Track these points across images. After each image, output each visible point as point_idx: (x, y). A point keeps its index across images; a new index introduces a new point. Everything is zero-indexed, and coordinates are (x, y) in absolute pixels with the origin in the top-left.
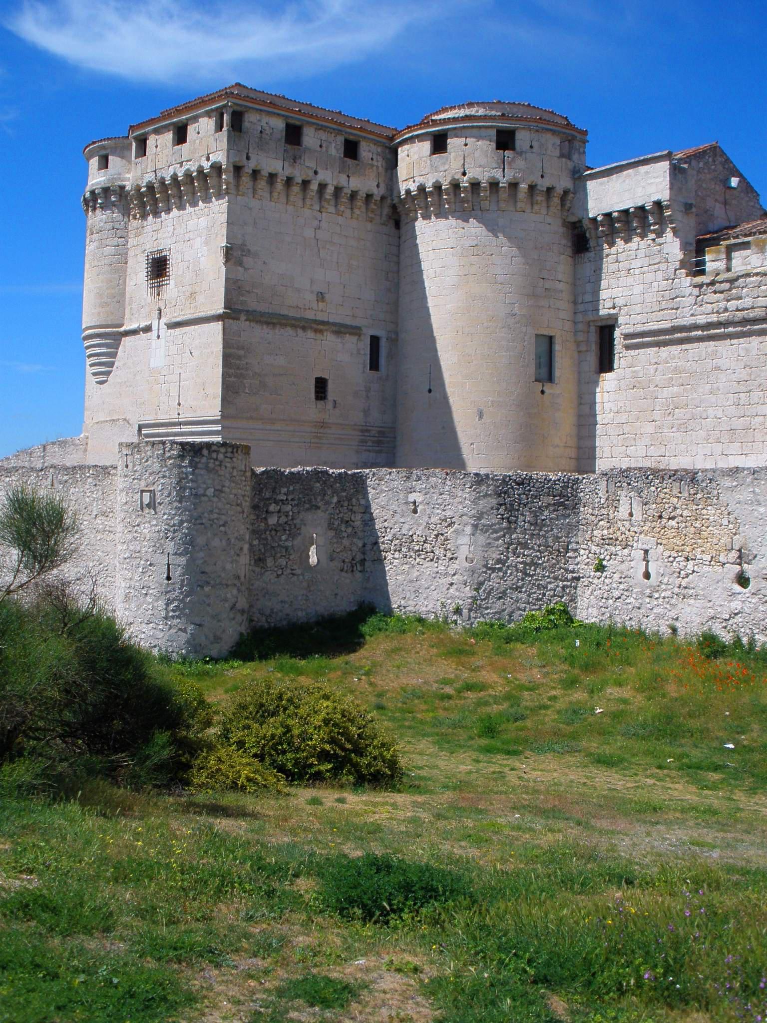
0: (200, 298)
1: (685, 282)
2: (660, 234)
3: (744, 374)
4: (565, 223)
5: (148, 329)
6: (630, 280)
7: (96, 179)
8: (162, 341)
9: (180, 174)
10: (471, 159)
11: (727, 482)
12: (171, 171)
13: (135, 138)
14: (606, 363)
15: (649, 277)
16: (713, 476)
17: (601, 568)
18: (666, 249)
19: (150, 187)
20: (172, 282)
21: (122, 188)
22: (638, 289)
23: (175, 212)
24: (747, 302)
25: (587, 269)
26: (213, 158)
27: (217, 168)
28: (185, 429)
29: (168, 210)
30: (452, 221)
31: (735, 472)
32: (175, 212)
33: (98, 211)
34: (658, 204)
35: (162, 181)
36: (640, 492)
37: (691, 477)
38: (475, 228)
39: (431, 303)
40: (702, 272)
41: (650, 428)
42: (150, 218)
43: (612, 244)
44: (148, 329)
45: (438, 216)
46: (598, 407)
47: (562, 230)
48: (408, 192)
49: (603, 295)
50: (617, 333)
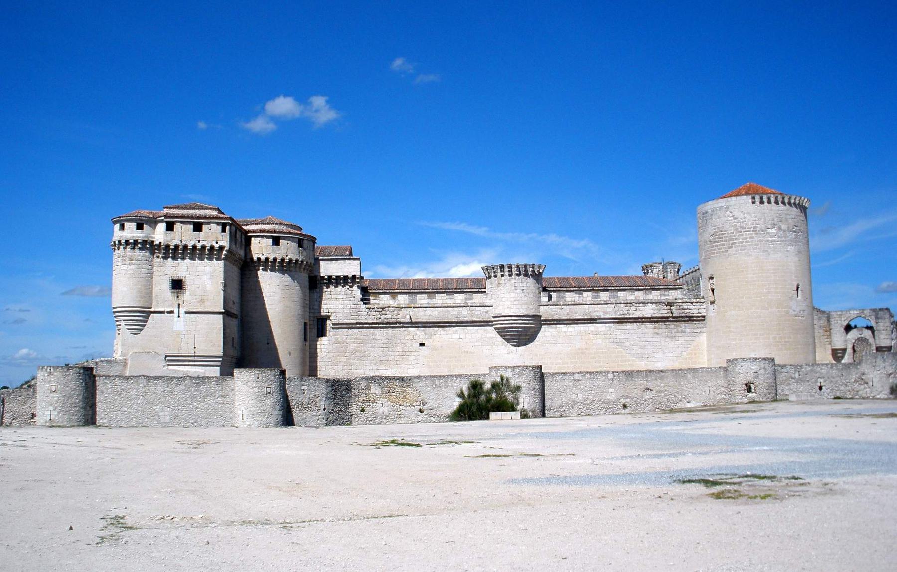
0: (207, 303)
1: (363, 307)
2: (351, 287)
3: (386, 341)
4: (310, 277)
5: (172, 312)
6: (337, 303)
7: (131, 232)
8: (182, 318)
9: (199, 246)
10: (288, 251)
11: (416, 380)
12: (193, 243)
13: (167, 222)
14: (322, 333)
15: (347, 302)
16: (411, 379)
17: (363, 410)
18: (354, 293)
19: (177, 247)
20: (187, 293)
21: (153, 242)
22: (340, 307)
23: (188, 261)
24: (389, 316)
25: (316, 296)
26: (220, 244)
27: (221, 248)
28: (197, 359)
29: (183, 259)
30: (277, 274)
31: (418, 377)
32: (188, 261)
33: (136, 250)
34: (354, 277)
35: (185, 247)
36: (379, 384)
37: (402, 379)
38: (287, 278)
39: (267, 306)
40: (369, 303)
41: (345, 359)
42: (170, 259)
43: (328, 287)
44: (172, 312)
45: (271, 271)
46: (319, 351)
47: (307, 279)
48: (259, 259)
49: (323, 307)
50: (328, 322)
